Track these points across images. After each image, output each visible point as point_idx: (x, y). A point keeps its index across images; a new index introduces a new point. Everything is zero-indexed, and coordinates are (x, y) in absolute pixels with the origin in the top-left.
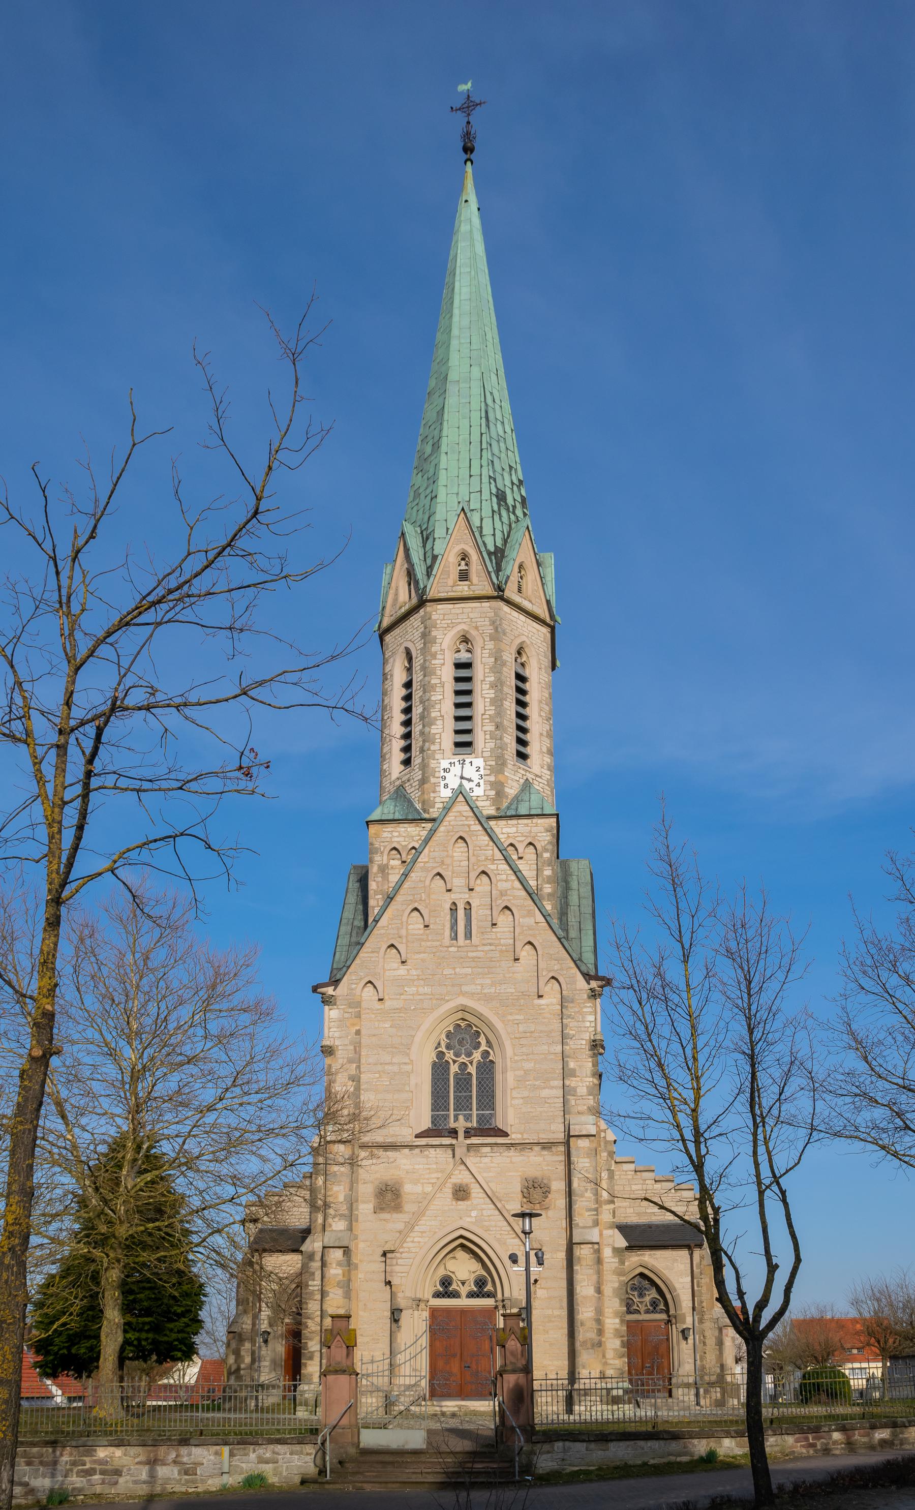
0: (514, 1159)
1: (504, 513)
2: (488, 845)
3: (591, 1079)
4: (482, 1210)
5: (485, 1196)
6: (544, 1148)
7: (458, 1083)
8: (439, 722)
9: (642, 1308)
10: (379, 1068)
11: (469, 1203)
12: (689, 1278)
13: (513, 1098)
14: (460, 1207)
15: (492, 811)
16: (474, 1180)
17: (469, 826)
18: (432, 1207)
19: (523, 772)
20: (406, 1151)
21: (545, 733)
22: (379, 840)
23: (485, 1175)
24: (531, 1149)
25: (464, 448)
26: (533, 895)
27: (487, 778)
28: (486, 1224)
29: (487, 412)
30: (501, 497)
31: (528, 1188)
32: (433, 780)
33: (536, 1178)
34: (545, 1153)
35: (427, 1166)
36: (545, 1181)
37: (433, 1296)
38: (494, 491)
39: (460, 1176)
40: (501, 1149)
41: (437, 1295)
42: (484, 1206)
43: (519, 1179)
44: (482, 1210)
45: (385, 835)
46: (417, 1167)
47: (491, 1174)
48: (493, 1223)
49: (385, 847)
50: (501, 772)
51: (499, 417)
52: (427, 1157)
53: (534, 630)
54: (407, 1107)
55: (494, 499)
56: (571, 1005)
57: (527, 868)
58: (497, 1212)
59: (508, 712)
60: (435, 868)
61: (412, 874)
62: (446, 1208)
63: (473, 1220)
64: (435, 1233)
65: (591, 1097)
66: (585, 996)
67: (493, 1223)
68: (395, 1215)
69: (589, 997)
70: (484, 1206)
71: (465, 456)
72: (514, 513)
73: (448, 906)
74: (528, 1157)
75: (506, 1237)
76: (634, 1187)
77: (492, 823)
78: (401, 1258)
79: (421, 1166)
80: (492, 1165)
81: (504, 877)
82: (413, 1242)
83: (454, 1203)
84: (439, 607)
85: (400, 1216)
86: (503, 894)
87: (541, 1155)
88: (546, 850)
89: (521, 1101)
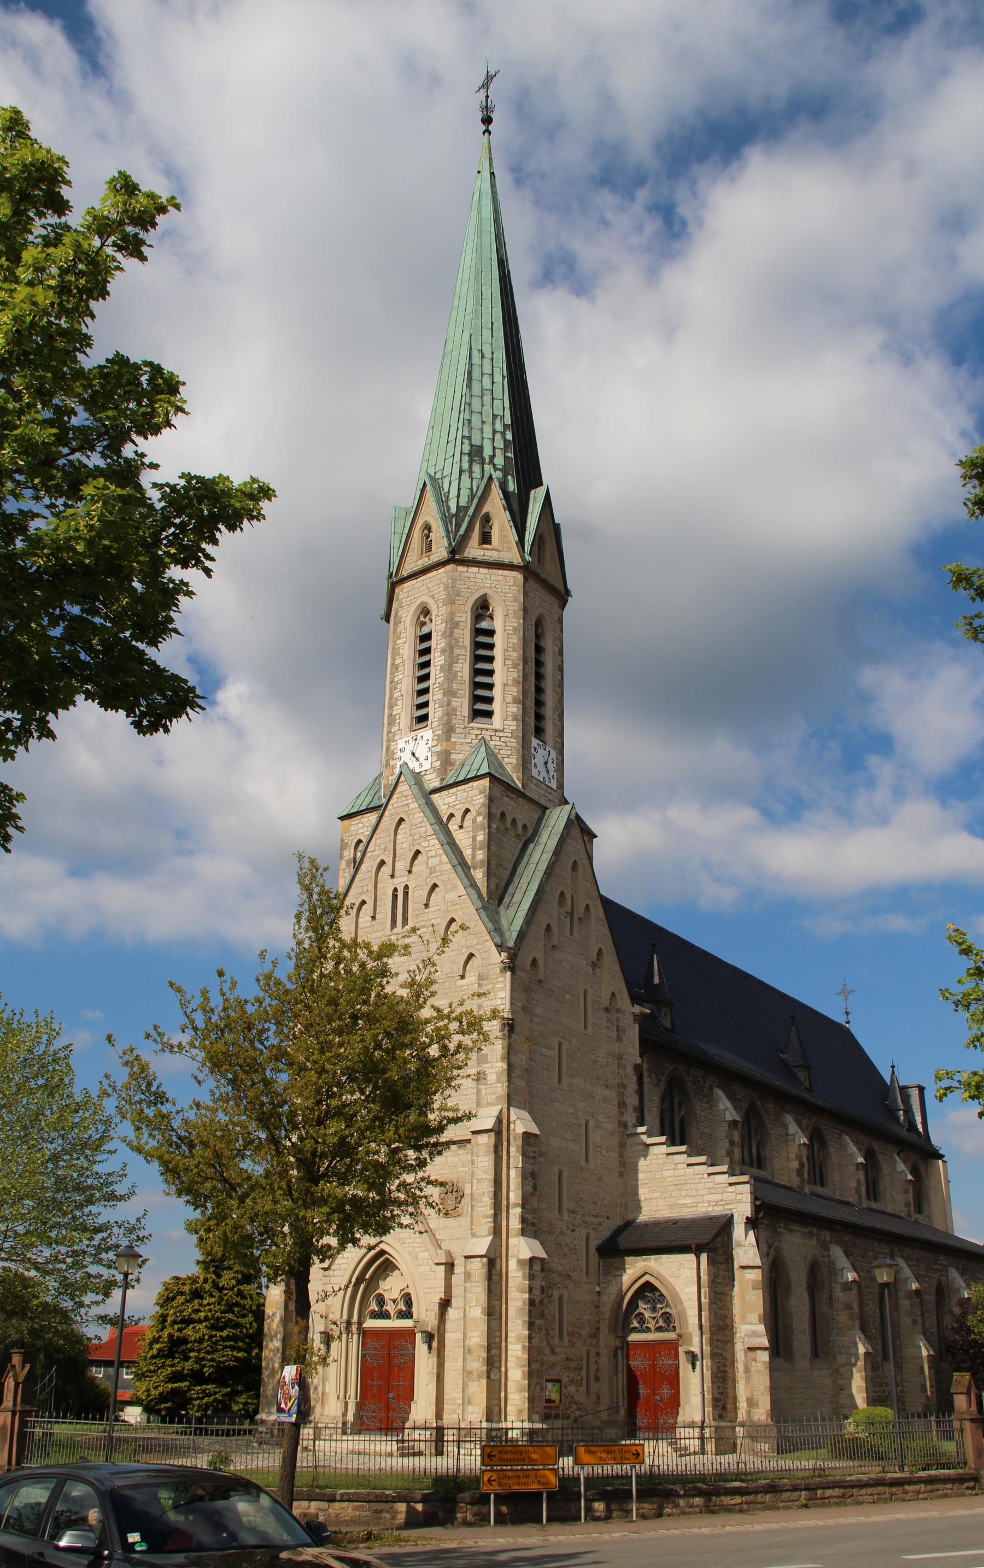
1: (477, 469)
2: (422, 822)
3: (500, 1064)
8: (399, 702)
9: (652, 1325)
12: (695, 1288)
15: (437, 784)
17: (408, 805)
19: (478, 732)
21: (510, 682)
22: (348, 834)
25: (447, 416)
26: (463, 866)
27: (434, 749)
29: (470, 373)
30: (476, 453)
32: (392, 763)
34: (461, 1152)
38: (466, 448)
41: (375, 1315)
45: (353, 828)
49: (352, 841)
50: (448, 739)
51: (487, 369)
53: (500, 578)
55: (466, 458)
56: (485, 982)
57: (463, 839)
59: (460, 674)
60: (379, 855)
61: (363, 867)
65: (500, 1085)
66: (498, 970)
69: (501, 972)
71: (446, 424)
72: (491, 462)
73: (390, 893)
75: (417, 1250)
76: (666, 1173)
77: (435, 797)
81: (433, 853)
84: (405, 585)
86: (432, 870)
87: (458, 1155)
88: (479, 814)
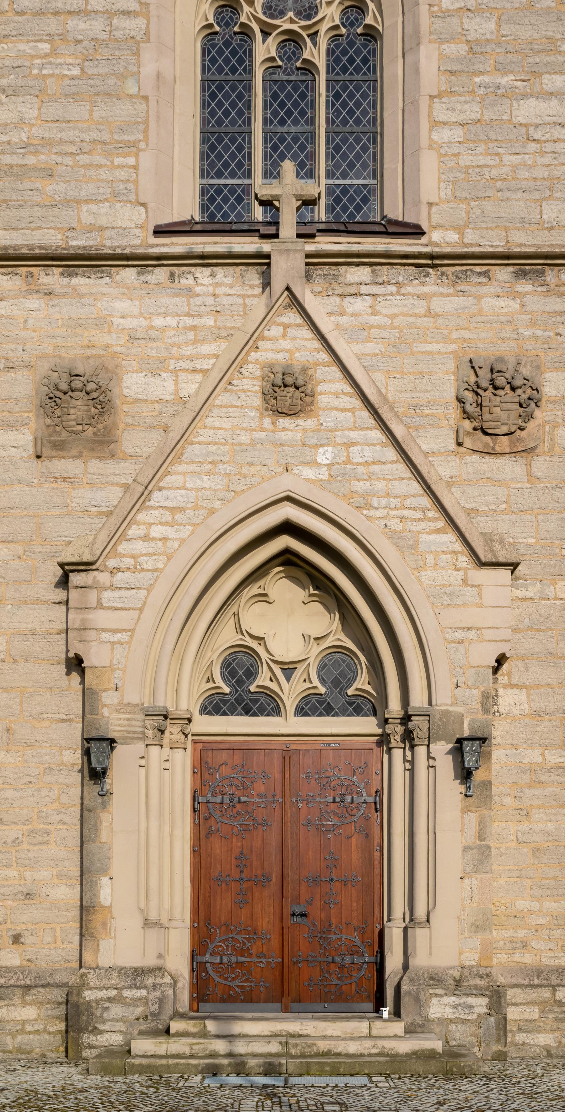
0: (438, 305)
4: (350, 444)
5: (356, 403)
6: (521, 274)
7: (275, 96)
10: (53, 25)
11: (310, 423)
13: (436, 124)
14: (284, 436)
16: (324, 356)
18: (203, 435)
20: (129, 275)
23: (358, 348)
24: (486, 274)
28: (360, 486)
31: (476, 390)
33: (501, 359)
34: (525, 287)
35: (189, 321)
36: (525, 371)
37: (205, 710)
39: (286, 344)
40: (403, 274)
42: (354, 435)
43: (451, 365)
44: (350, 444)
46: (159, 322)
47: (370, 348)
48: (381, 486)
52: (190, 292)
54: (134, 145)
58: (391, 454)
62: (244, 438)
63: (323, 474)
64: (212, 511)
67: (381, 486)
68: (96, 466)
70: (354, 435)
74: (478, 298)
75: (417, 527)
78: (113, 588)
79: (172, 321)
80: (374, 320)
82: (146, 538)
83: (267, 422)
85: (110, 466)
87: (515, 295)
89: (458, 133)
